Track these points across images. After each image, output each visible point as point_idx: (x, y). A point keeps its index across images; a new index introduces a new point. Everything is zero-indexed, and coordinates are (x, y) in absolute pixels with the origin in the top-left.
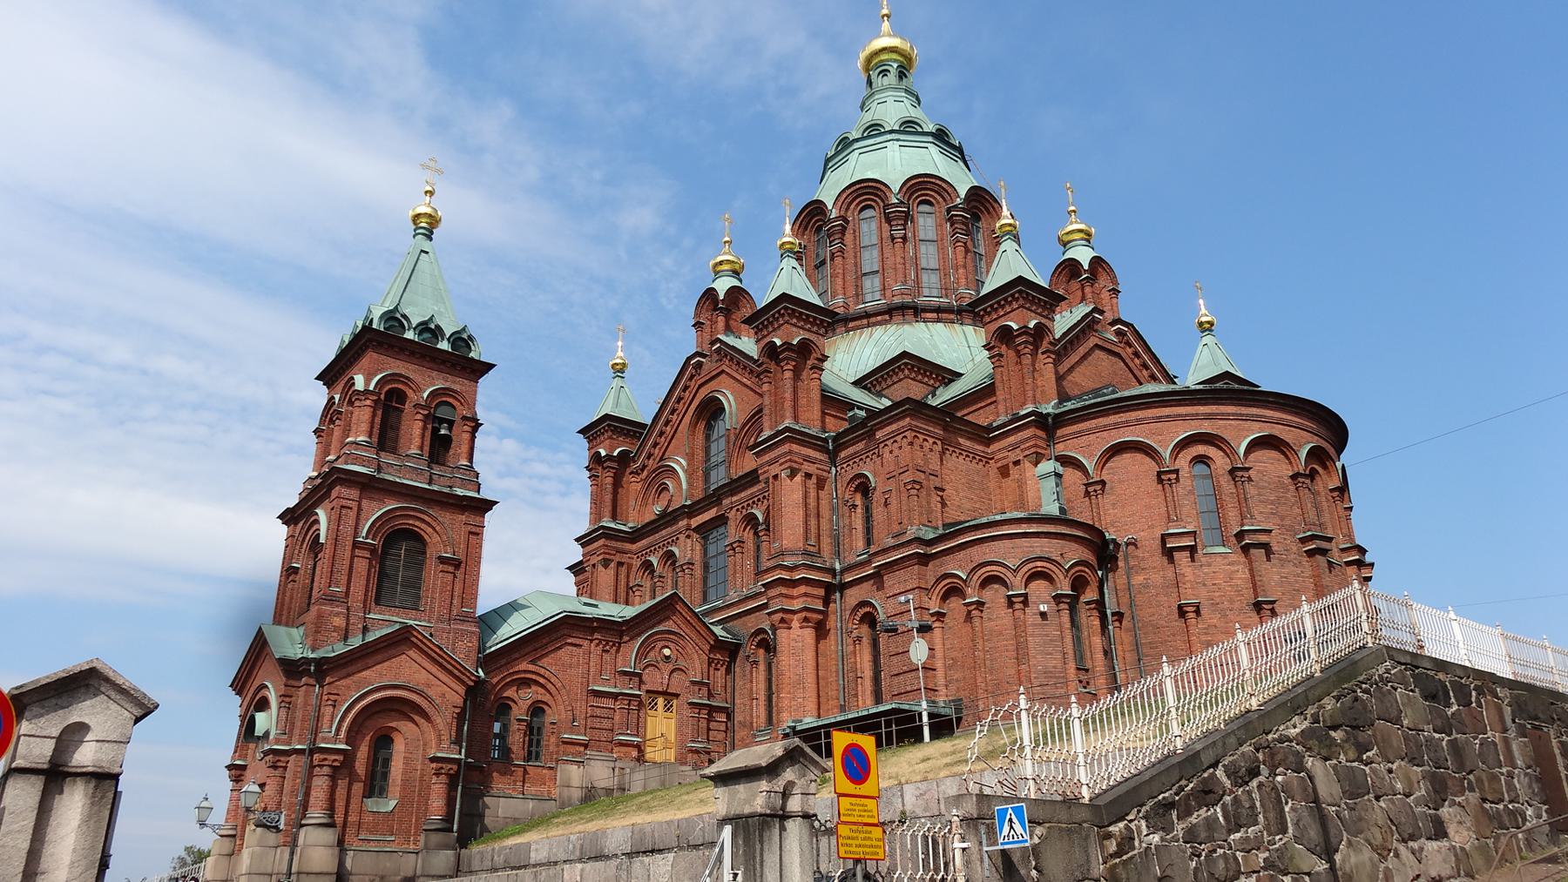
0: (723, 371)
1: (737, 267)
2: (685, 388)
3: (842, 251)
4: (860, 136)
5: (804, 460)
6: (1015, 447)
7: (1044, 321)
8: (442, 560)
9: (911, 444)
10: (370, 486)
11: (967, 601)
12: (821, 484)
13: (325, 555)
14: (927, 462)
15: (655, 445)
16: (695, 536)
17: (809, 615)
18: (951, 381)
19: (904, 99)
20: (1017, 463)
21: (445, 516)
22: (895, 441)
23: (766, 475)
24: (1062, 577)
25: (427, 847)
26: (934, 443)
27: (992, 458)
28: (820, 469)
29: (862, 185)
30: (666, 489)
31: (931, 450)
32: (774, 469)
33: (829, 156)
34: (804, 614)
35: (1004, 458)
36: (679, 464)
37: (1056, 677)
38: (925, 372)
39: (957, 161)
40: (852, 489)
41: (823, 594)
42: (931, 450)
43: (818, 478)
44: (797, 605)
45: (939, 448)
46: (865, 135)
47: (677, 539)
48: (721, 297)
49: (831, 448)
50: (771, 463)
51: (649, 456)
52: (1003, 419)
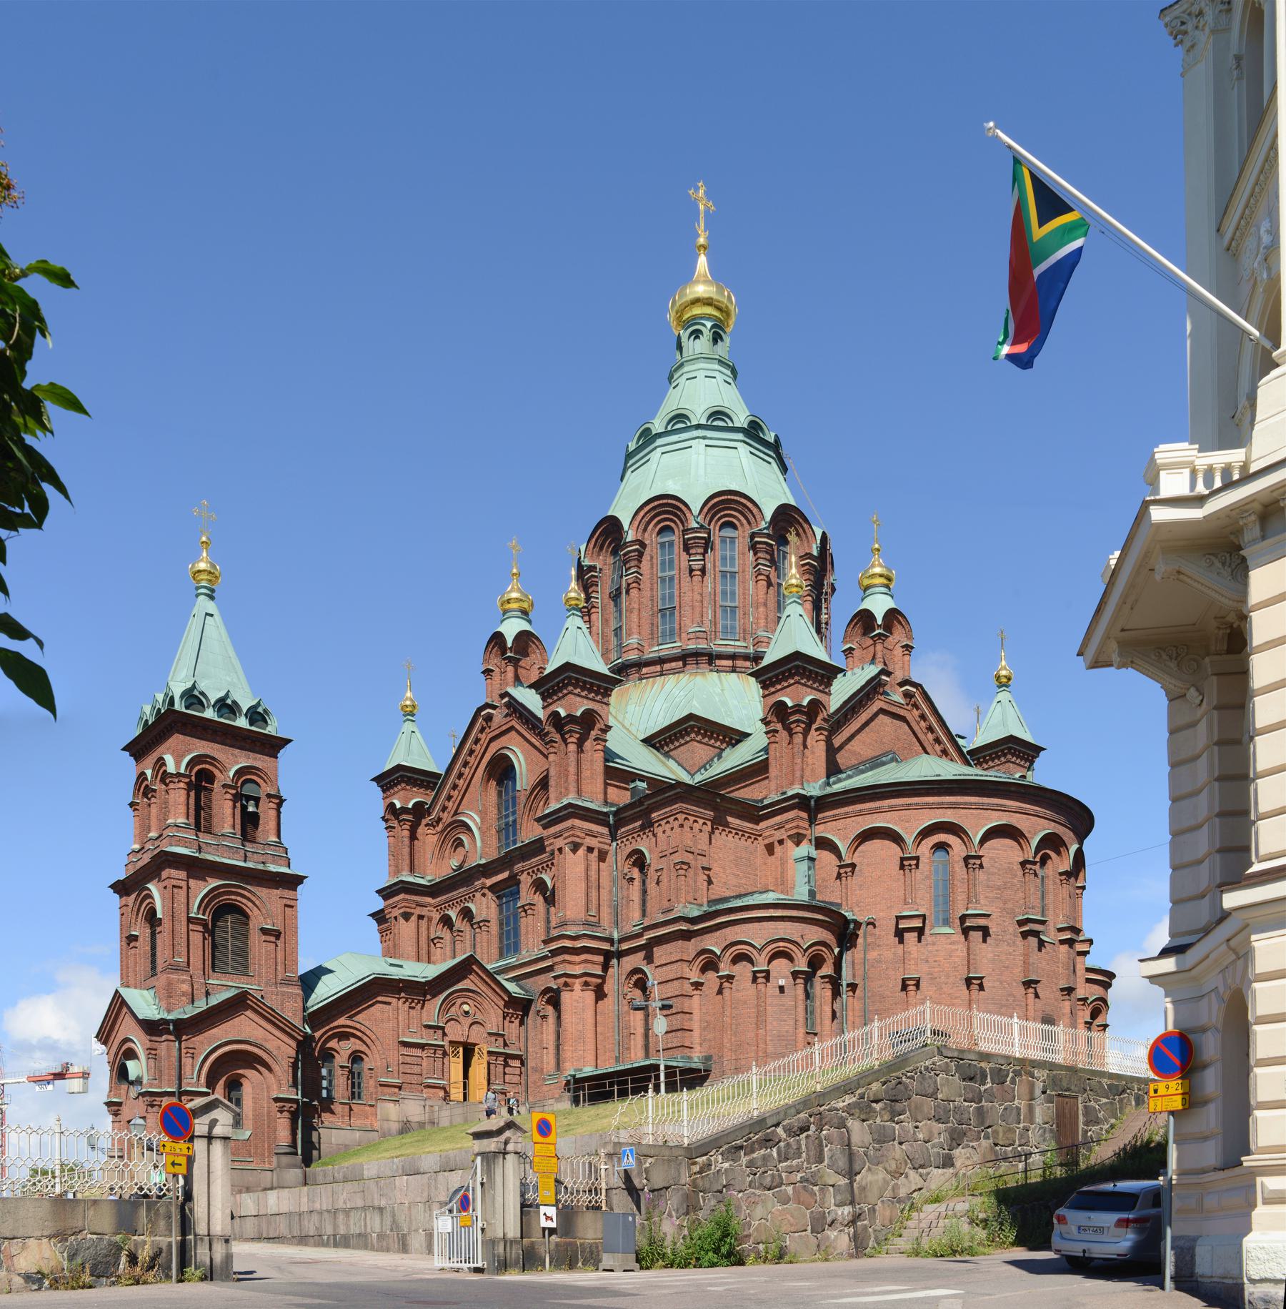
1: (526, 605)
2: (477, 741)
5: (587, 834)
6: (780, 827)
7: (819, 696)
8: (264, 931)
9: (681, 826)
10: (196, 868)
11: (720, 974)
12: (602, 856)
13: (166, 926)
14: (696, 842)
17: (588, 979)
18: (738, 742)
20: (781, 842)
21: (263, 892)
22: (668, 822)
23: (551, 847)
24: (800, 955)
25: (279, 1166)
26: (704, 824)
27: (760, 835)
28: (601, 843)
29: (661, 502)
31: (701, 831)
32: (559, 843)
33: (630, 450)
34: (585, 979)
35: (771, 836)
37: (787, 1040)
38: (712, 733)
39: (770, 463)
40: (631, 863)
42: (701, 831)
43: (600, 851)
44: (578, 970)
45: (708, 828)
48: (509, 645)
49: (612, 822)
50: (557, 836)
52: (774, 797)
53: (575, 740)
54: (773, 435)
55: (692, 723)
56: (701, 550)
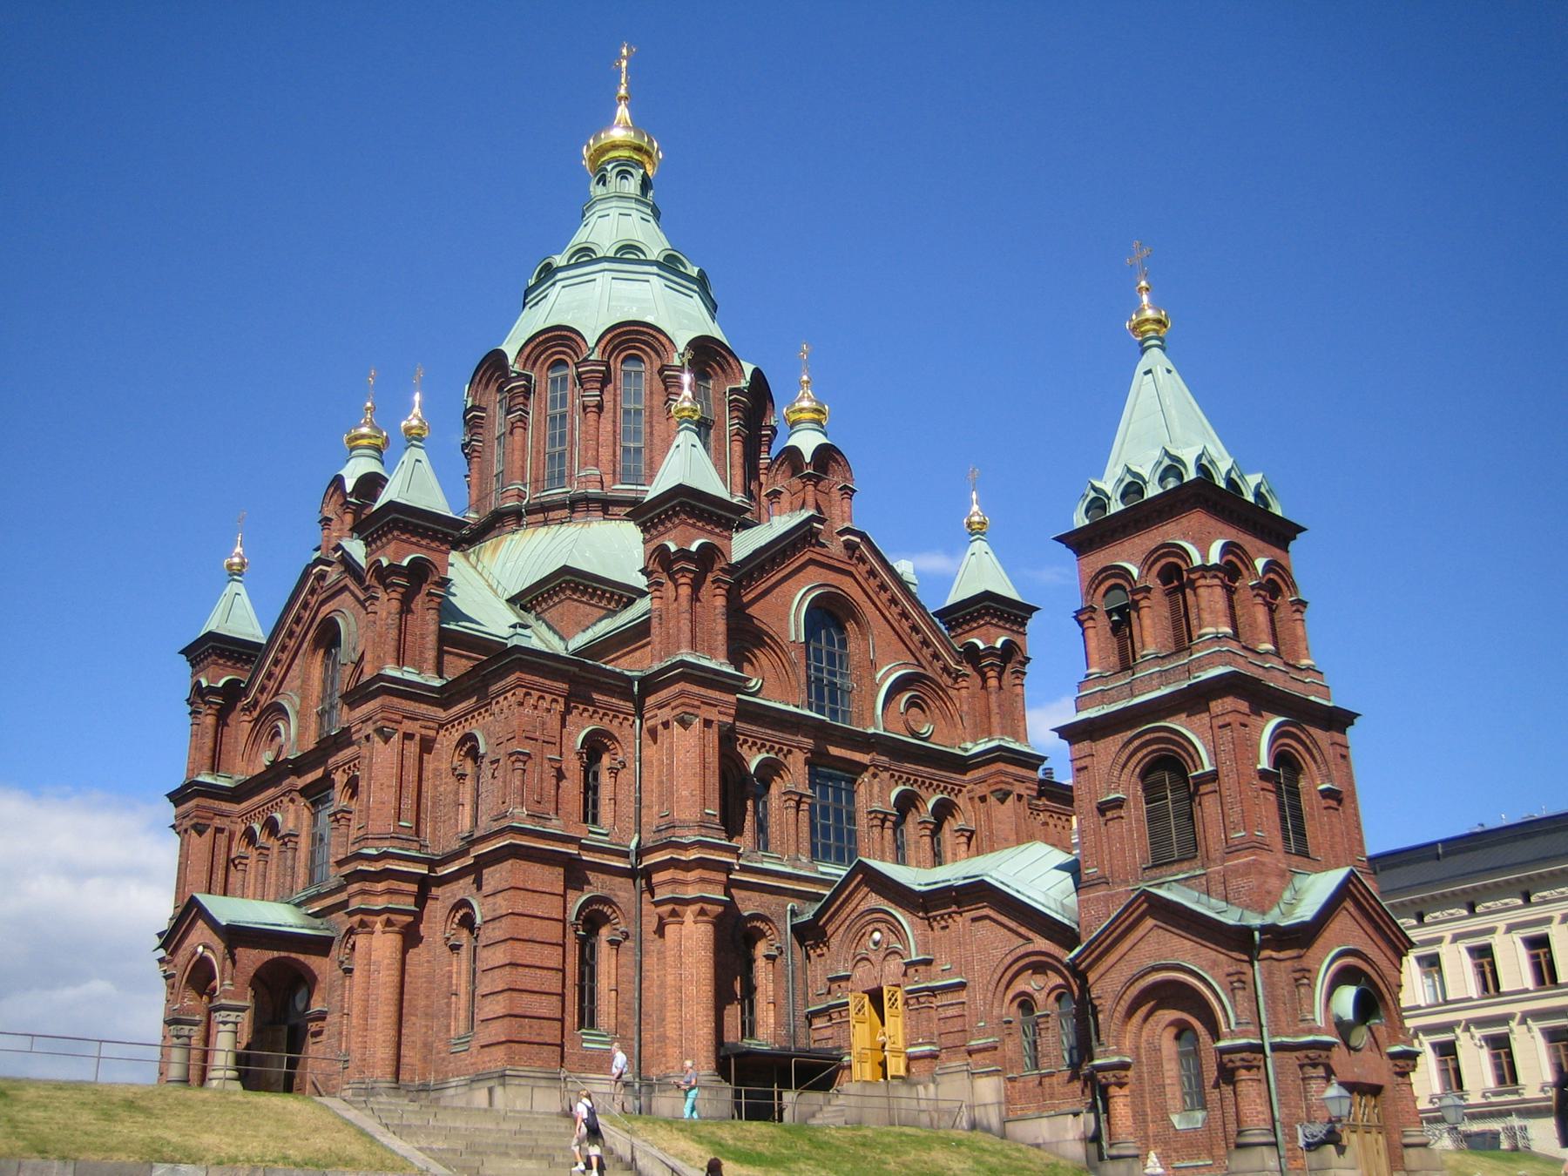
0: (345, 588)
1: (379, 442)
3: (523, 420)
4: (565, 263)
5: (404, 717)
12: (427, 746)
15: (269, 676)
16: (301, 801)
17: (394, 917)
19: (634, 213)
22: (506, 698)
26: (554, 700)
28: (425, 728)
30: (278, 733)
36: (290, 702)
40: (462, 753)
41: (416, 890)
43: (423, 739)
44: (379, 903)
45: (560, 707)
46: (572, 261)
47: (281, 801)
51: (262, 689)
53: (399, 596)
54: (696, 269)
55: (568, 578)
56: (599, 385)
